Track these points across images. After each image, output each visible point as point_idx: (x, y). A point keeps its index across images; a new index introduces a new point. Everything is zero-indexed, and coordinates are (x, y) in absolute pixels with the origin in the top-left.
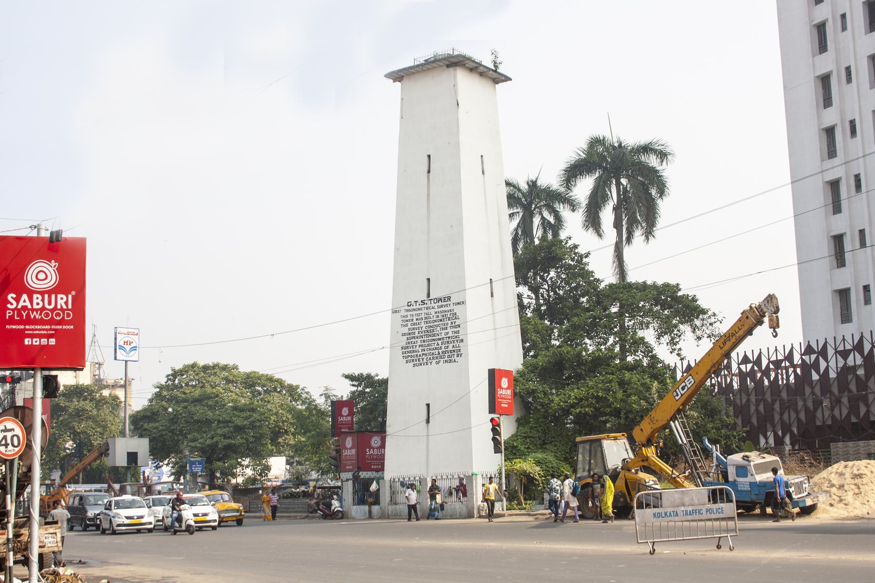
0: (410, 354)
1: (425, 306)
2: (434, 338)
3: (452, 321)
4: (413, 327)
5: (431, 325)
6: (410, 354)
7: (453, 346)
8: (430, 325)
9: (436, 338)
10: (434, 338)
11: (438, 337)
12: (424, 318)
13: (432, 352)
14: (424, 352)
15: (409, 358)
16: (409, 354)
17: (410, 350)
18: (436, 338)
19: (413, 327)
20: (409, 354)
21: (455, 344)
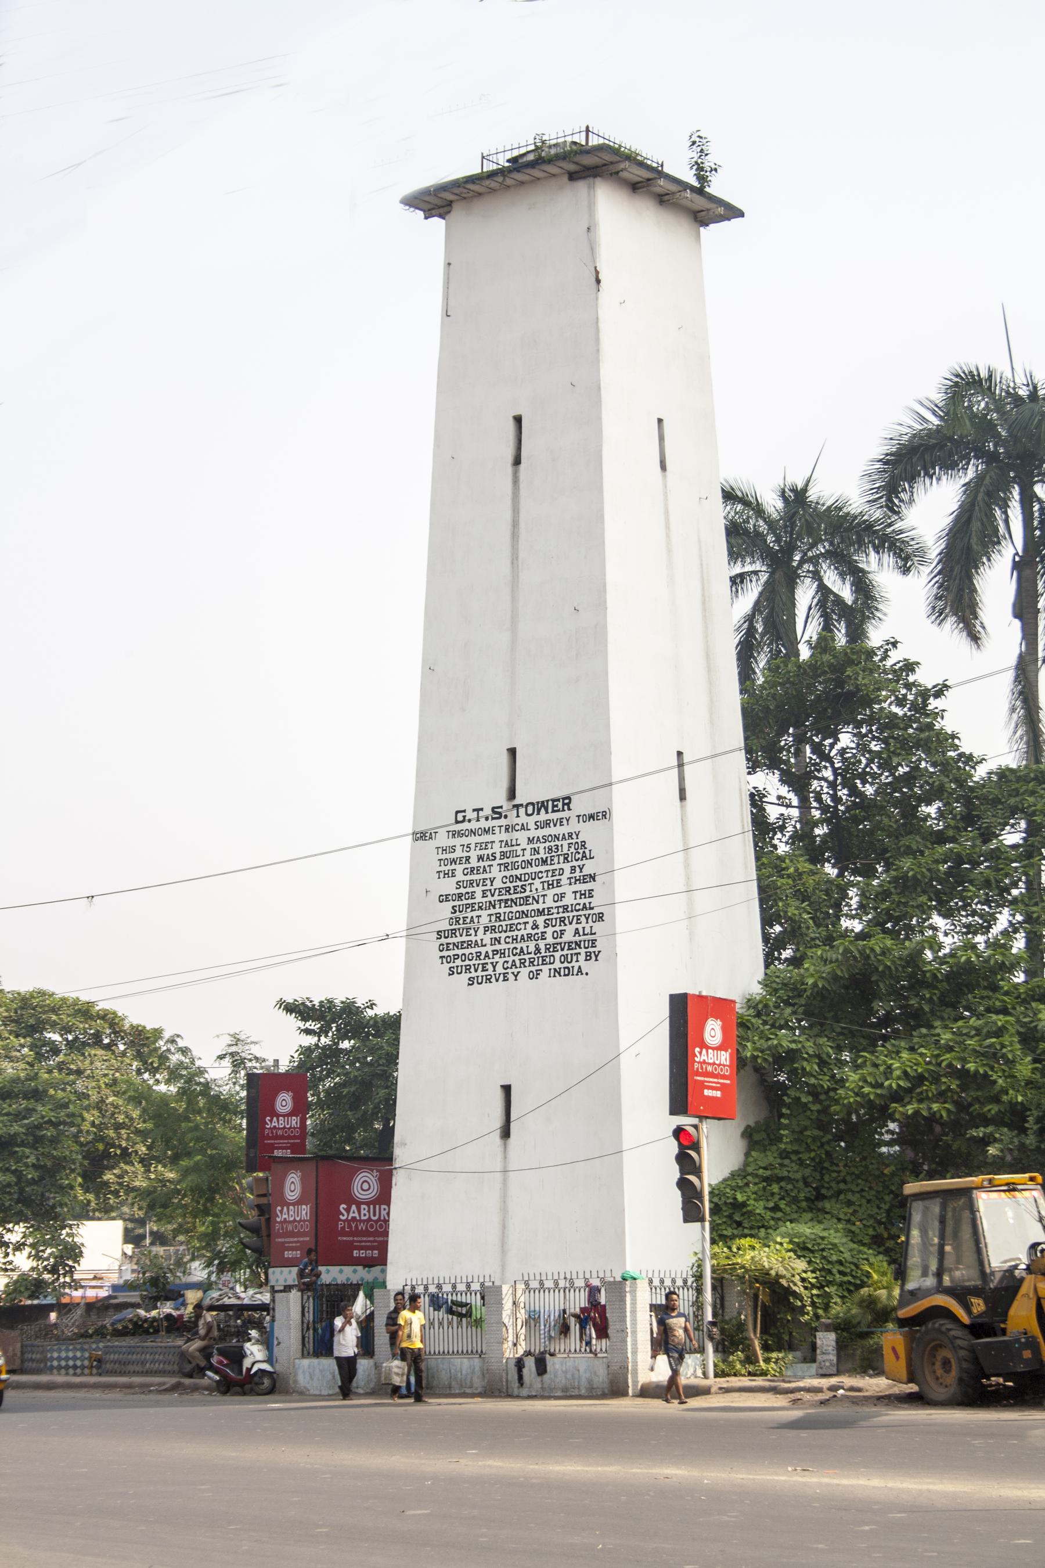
0: (460, 952)
1: (503, 822)
2: (524, 908)
3: (575, 863)
4: (469, 877)
5: (518, 872)
6: (460, 952)
7: (577, 932)
8: (514, 872)
9: (530, 908)
10: (524, 908)
11: (535, 906)
12: (498, 856)
13: (519, 946)
14: (498, 947)
15: (458, 962)
16: (456, 952)
17: (459, 939)
18: (530, 908)
19: (469, 877)
20: (456, 952)
21: (580, 927)
